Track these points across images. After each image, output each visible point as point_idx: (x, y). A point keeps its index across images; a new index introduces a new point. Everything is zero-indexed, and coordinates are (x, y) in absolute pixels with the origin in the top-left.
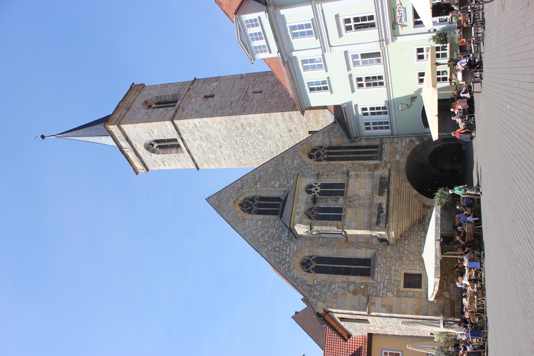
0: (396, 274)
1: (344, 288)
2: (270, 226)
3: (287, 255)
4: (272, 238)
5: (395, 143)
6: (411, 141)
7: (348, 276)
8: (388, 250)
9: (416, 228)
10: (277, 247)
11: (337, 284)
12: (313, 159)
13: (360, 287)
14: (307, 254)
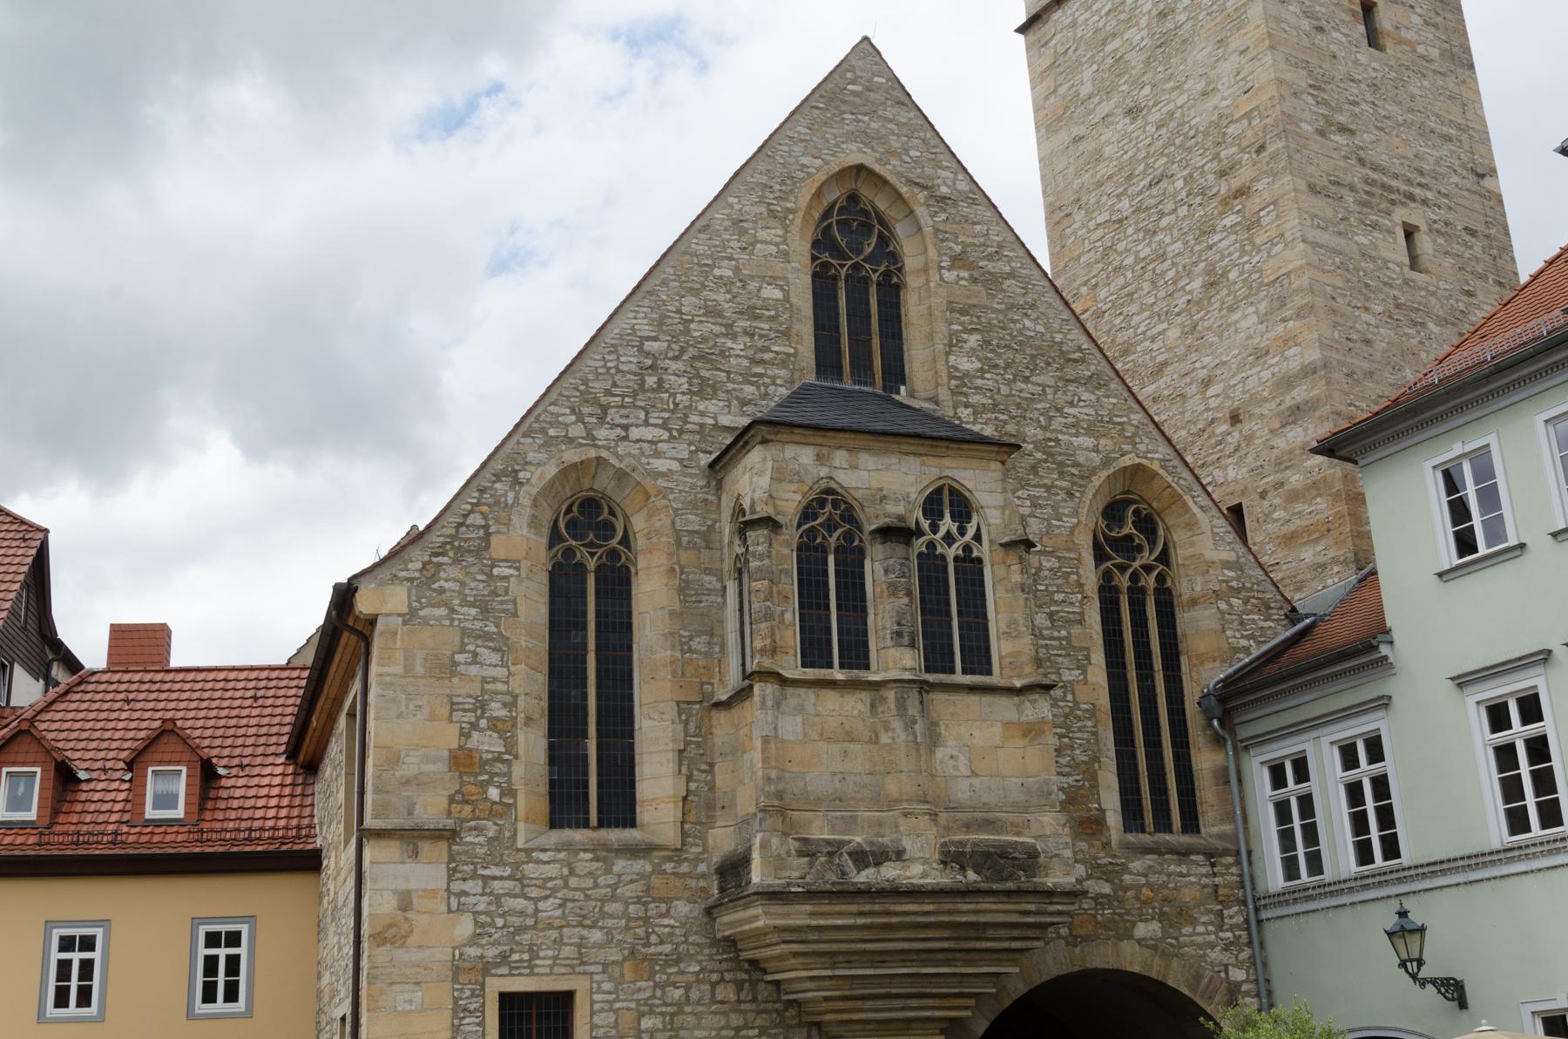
0: (567, 951)
1: (483, 706)
2: (760, 344)
3: (626, 428)
4: (702, 357)
5: (1220, 914)
6: (1233, 994)
7: (544, 723)
8: (682, 908)
10: (660, 381)
11: (500, 672)
12: (1102, 523)
13: (489, 782)
14: (638, 523)
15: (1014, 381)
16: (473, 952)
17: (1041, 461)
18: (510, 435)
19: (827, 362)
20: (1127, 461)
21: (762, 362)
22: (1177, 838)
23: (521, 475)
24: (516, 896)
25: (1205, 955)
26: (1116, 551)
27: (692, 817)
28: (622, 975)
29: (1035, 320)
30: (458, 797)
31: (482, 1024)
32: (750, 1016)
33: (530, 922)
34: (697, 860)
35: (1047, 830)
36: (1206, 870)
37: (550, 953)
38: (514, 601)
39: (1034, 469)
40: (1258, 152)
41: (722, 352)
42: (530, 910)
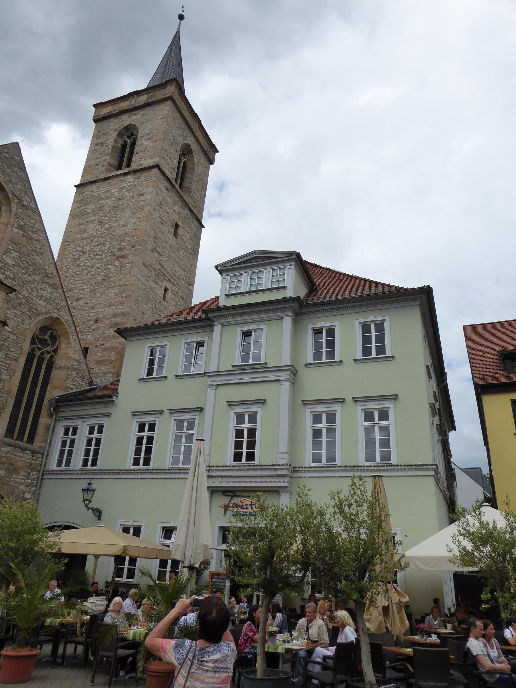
5: (29, 473)
15: (25, 274)
17: (23, 303)
20: (54, 315)
25: (18, 486)
29: (41, 258)
39: (20, 304)
40: (132, 247)
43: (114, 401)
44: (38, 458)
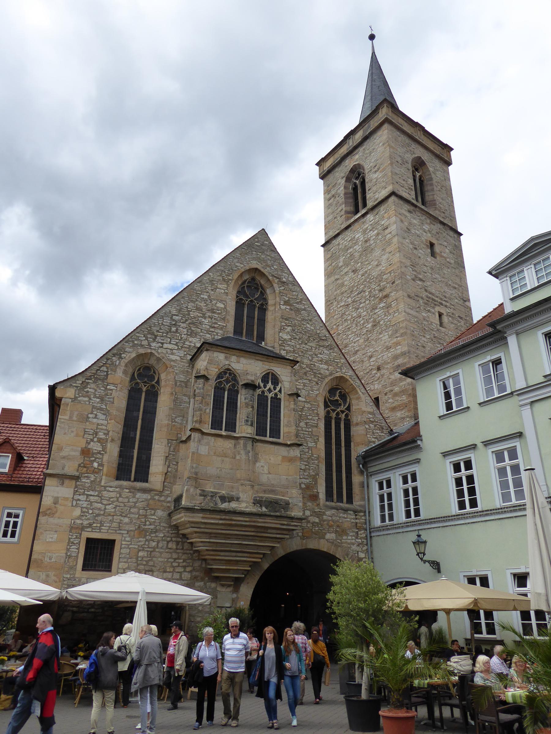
0: (115, 525)
1: (96, 434)
2: (214, 321)
3: (162, 344)
4: (193, 323)
5: (357, 533)
7: (119, 442)
8: (160, 513)
9: (197, 564)
10: (177, 330)
11: (105, 422)
12: (328, 395)
13: (94, 461)
14: (163, 376)
15: (302, 344)
16: (79, 522)
17: (308, 371)
18: (121, 341)
19: (238, 330)
20: (338, 375)
21: (214, 327)
22: (344, 505)
23: (123, 355)
24: (98, 503)
25: (351, 547)
26: (332, 405)
27: (168, 481)
28: (134, 535)
30: (82, 465)
31: (78, 549)
32: (180, 554)
33: (102, 513)
34: (168, 496)
35: (294, 497)
36: (354, 517)
37: (108, 525)
38: (113, 398)
39: (305, 374)
41: (200, 323)
42: (103, 509)
43: (419, 445)
44: (361, 516)
